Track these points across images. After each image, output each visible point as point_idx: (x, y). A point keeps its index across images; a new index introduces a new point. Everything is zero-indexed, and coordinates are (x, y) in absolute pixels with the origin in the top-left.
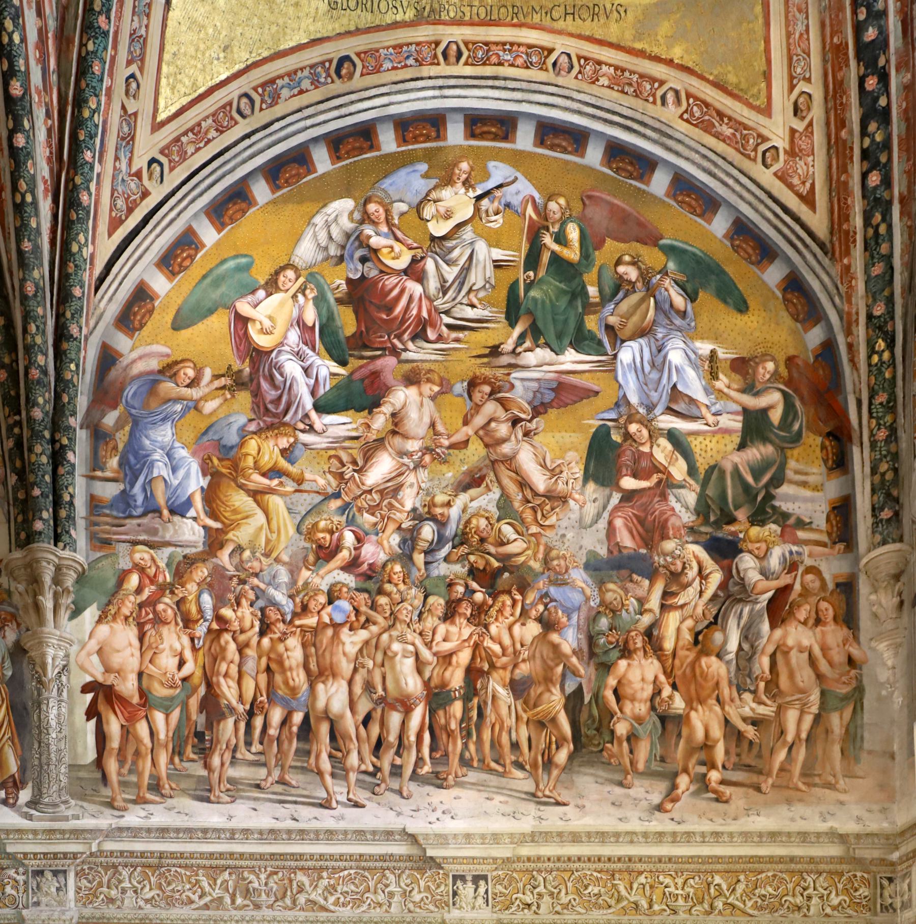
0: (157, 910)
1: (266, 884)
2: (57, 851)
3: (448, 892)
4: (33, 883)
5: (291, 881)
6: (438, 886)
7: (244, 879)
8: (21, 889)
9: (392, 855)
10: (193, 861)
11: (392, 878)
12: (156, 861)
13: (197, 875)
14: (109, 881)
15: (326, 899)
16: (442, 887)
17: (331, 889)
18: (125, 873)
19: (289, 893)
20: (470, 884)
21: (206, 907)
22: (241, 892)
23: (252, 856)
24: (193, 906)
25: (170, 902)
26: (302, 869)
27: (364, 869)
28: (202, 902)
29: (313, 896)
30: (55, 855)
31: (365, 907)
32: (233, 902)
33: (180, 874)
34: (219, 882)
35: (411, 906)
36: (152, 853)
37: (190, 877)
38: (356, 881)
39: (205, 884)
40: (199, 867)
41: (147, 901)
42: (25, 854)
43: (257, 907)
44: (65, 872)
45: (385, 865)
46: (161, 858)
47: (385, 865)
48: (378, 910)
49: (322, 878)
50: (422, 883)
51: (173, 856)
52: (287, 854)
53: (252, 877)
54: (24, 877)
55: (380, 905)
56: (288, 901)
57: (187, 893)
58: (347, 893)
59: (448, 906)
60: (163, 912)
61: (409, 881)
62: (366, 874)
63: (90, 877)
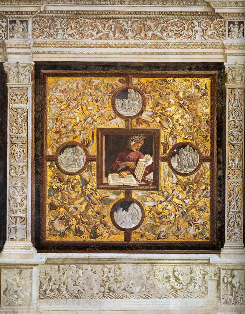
0: (74, 40)
1: (131, 27)
2: (22, 10)
3: (226, 30)
4: (10, 27)
5: (144, 25)
6: (221, 27)
7: (120, 24)
8: (4, 30)
9: (197, 12)
10: (94, 16)
11: (196, 23)
12: (75, 15)
13: (96, 22)
14: (50, 25)
15: (162, 34)
16: (223, 28)
17: (165, 29)
18: (58, 21)
19: (143, 31)
20: (237, 26)
21: (100, 38)
22: (118, 31)
23: (124, 13)
24: (94, 38)
25: (81, 36)
26: (150, 19)
27: (182, 19)
28: (98, 36)
29: (155, 33)
30: (22, 13)
31: (182, 37)
32: (114, 35)
33: (87, 22)
34: (107, 26)
35: (206, 37)
36: (72, 11)
37: (92, 23)
38: (178, 25)
39: (100, 27)
40: (96, 18)
41: (69, 35)
42: (6, 12)
43: (127, 38)
44: (27, 21)
45: (193, 17)
46: (77, 14)
47: (193, 17)
48: (189, 39)
49: (160, 23)
50: (212, 26)
51: (84, 12)
52: (142, 12)
53: (124, 23)
54: (6, 24)
55: (190, 37)
56: (142, 35)
57: (90, 31)
58: (173, 31)
59: (226, 37)
60: (77, 40)
61: (205, 25)
62: (183, 21)
63: (40, 24)
